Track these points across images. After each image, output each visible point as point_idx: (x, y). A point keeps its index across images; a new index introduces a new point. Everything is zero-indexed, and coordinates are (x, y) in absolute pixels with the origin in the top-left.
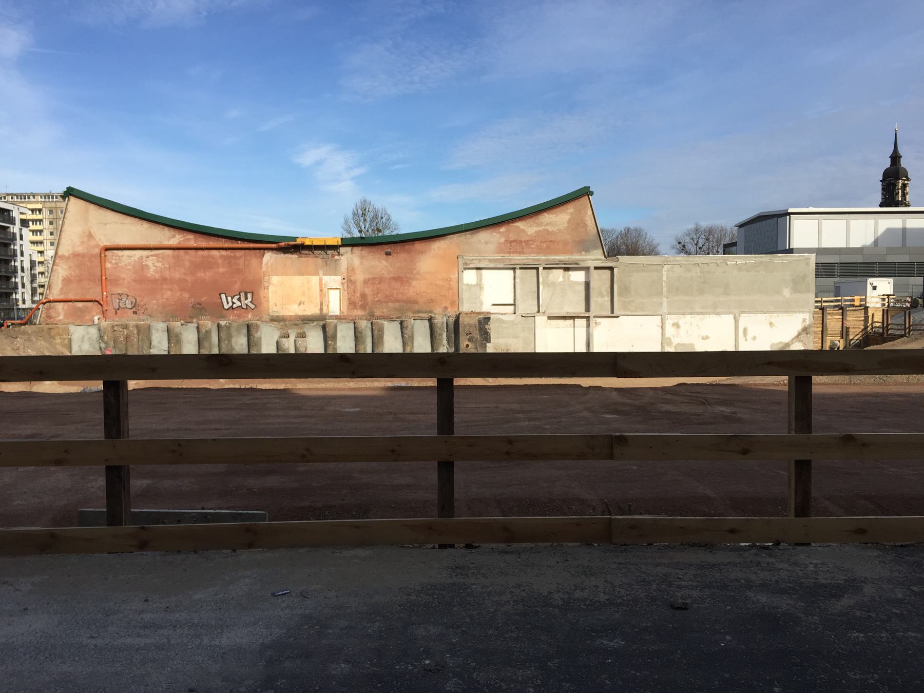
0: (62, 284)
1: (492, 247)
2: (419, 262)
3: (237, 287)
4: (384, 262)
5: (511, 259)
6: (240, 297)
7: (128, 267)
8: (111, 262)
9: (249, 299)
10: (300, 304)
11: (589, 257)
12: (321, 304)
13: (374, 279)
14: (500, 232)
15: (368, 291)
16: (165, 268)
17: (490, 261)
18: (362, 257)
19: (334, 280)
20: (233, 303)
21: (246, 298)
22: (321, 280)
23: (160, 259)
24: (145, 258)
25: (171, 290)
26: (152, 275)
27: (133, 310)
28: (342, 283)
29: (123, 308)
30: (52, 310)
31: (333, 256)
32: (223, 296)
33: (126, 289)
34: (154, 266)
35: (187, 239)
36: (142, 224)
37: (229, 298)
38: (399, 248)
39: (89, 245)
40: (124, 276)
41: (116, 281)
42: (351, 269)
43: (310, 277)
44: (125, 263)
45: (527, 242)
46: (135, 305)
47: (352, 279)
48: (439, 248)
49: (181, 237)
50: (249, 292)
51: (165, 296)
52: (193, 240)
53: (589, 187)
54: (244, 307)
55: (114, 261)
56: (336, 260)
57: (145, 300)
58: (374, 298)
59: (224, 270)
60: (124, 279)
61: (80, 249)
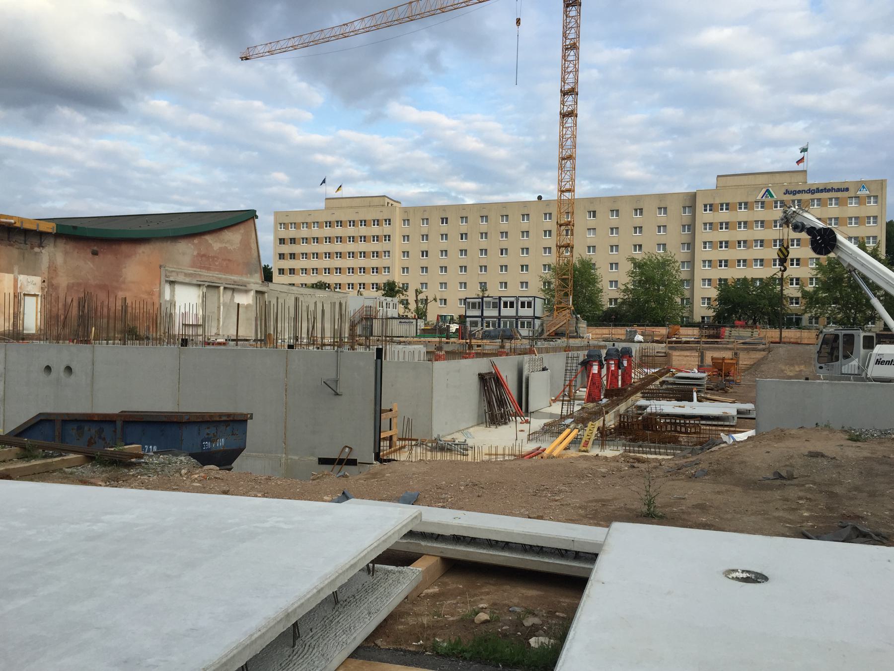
1: (187, 259)
2: (125, 267)
4: (89, 263)
5: (200, 275)
11: (252, 280)
13: (79, 284)
14: (193, 244)
17: (186, 275)
18: (66, 253)
19: (32, 283)
22: (16, 281)
28: (42, 288)
38: (106, 247)
45: (213, 257)
47: (54, 282)
48: (143, 252)
53: (255, 211)
56: (36, 253)
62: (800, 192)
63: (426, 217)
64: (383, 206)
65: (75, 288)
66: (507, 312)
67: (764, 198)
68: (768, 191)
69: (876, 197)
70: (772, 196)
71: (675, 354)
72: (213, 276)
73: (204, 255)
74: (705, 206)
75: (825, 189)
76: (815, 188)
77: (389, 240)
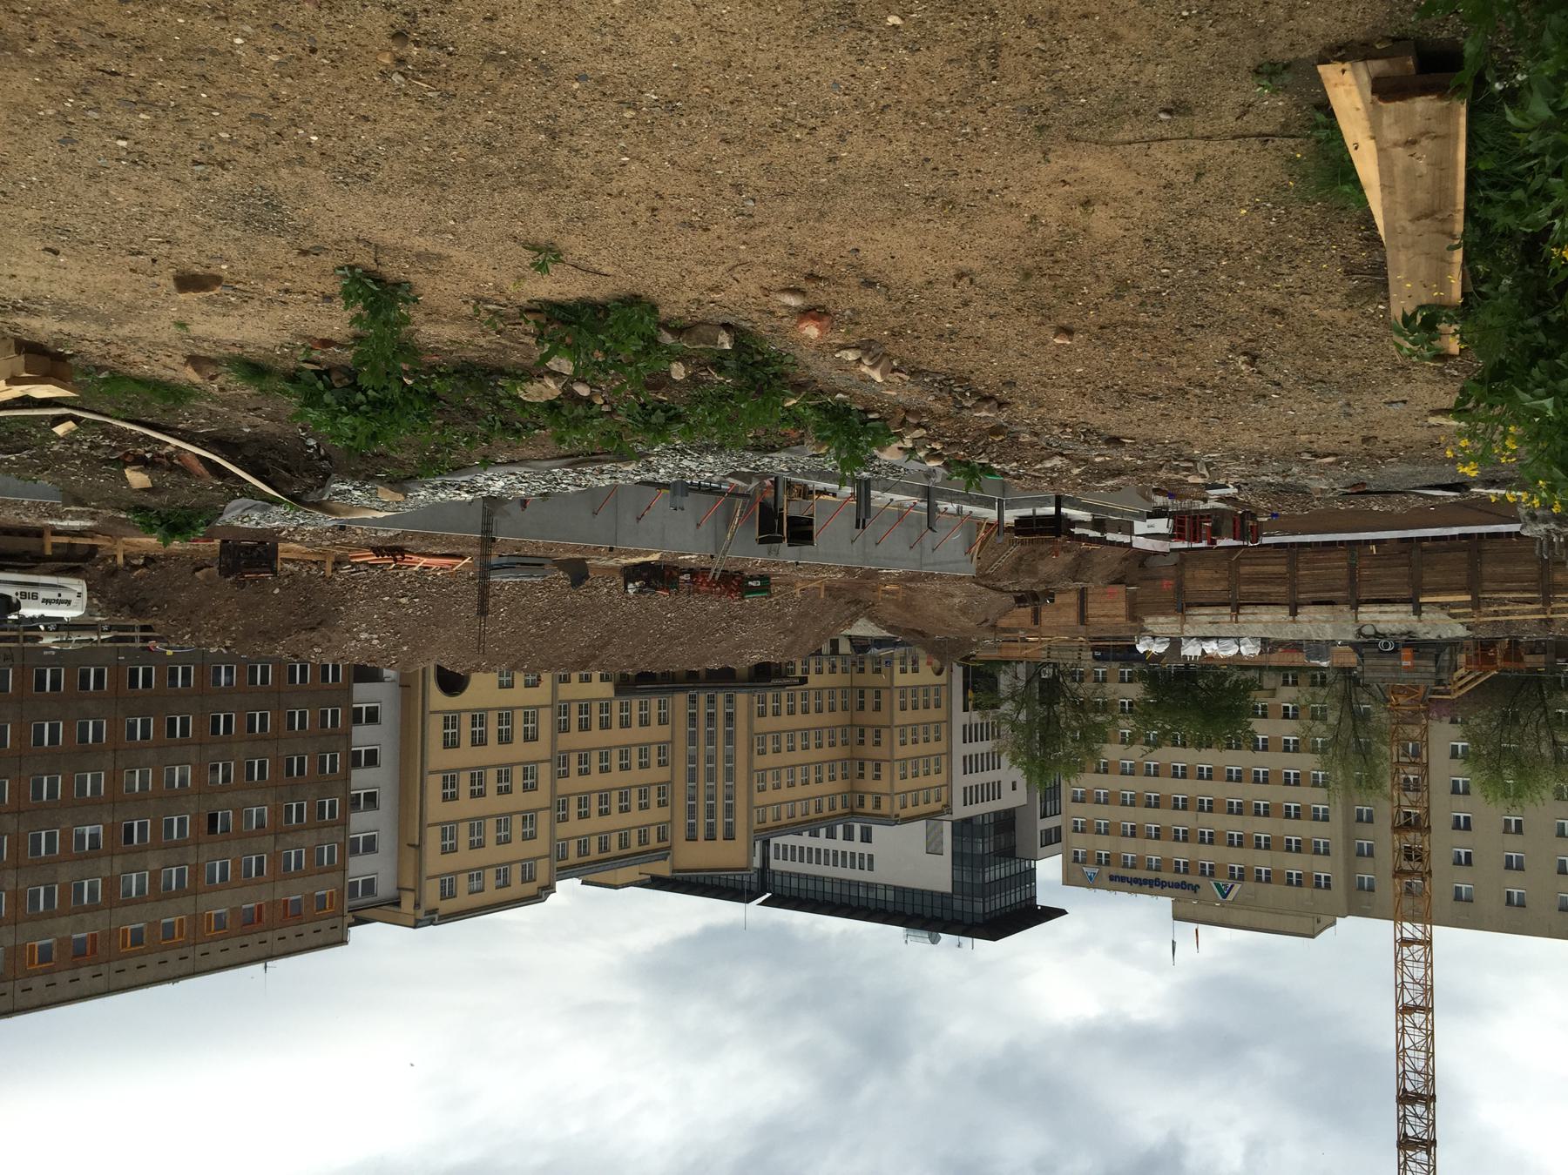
62: (1177, 886)
67: (1230, 885)
68: (1225, 896)
69: (1076, 860)
70: (1217, 885)
71: (1121, 619)
74: (1328, 886)
75: (1141, 885)
76: (1155, 888)
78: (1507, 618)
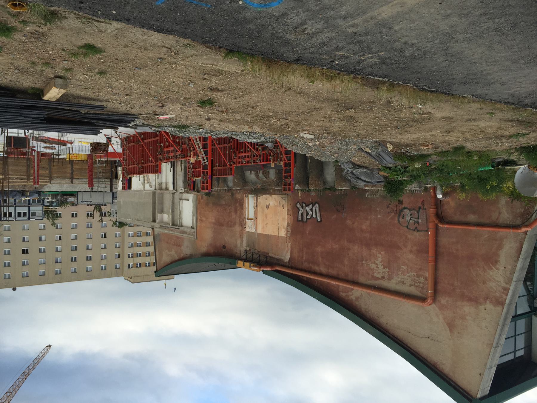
0: (498, 256)
1: (186, 243)
3: (309, 228)
5: (180, 233)
6: (307, 216)
7: (405, 268)
8: (426, 279)
9: (300, 213)
10: (269, 205)
12: (257, 205)
13: (231, 226)
14: (183, 254)
15: (234, 216)
16: (366, 261)
18: (236, 246)
20: (311, 210)
21: (302, 214)
22: (256, 230)
23: (371, 272)
24: (386, 276)
25: (362, 230)
26: (380, 253)
27: (403, 206)
29: (414, 209)
30: (518, 211)
31: (250, 250)
32: (319, 219)
33: (409, 236)
34: (378, 265)
35: (345, 292)
36: (387, 324)
37: (314, 216)
39: (454, 313)
40: (411, 256)
41: (422, 250)
42: (241, 236)
43: (262, 233)
44: (408, 275)
46: (400, 213)
47: (241, 228)
49: (350, 296)
50: (300, 221)
51: (368, 222)
52: (340, 290)
54: (304, 205)
55: (422, 279)
57: (389, 218)
58: (231, 209)
59: (317, 249)
60: (411, 252)
61: (467, 308)
63: (103, 271)
64: (134, 277)
65: (232, 224)
66: (25, 209)
72: (175, 232)
73: (179, 246)
77: (129, 255)
78: (12, 184)
